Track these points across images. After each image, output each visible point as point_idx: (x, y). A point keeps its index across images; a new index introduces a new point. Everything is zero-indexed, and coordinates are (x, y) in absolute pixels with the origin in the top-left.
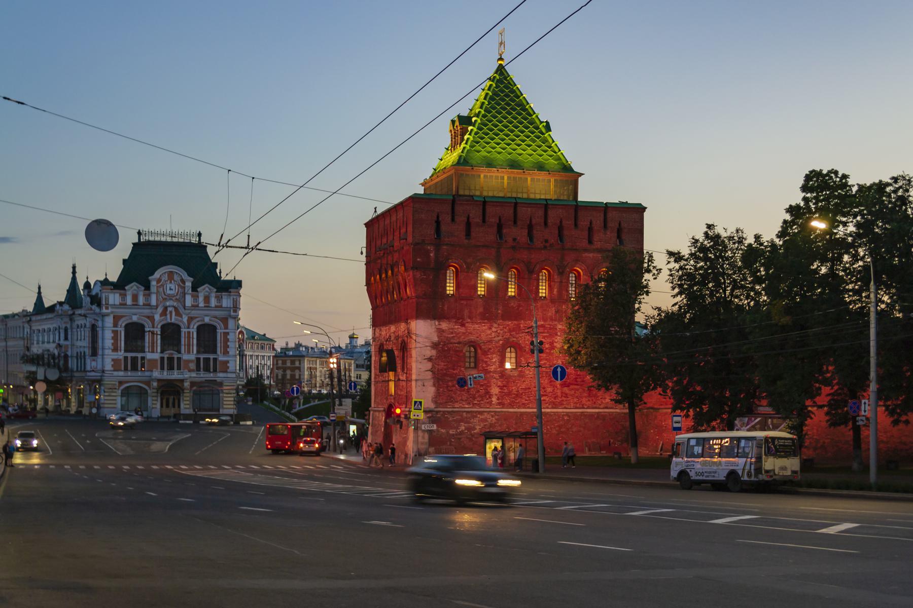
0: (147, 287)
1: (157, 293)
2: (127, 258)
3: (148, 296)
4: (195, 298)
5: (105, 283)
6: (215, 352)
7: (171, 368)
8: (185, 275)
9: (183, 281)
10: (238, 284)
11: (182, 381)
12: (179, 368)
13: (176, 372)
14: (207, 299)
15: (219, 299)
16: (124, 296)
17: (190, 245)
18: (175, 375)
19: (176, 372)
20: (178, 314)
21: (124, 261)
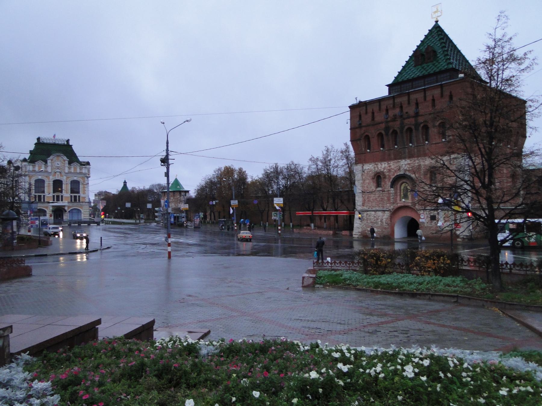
0: (46, 162)
1: (52, 166)
2: (32, 149)
3: (46, 166)
4: (69, 168)
5: (25, 160)
6: (78, 192)
7: (58, 200)
8: (65, 158)
9: (64, 161)
10: (88, 163)
11: (64, 206)
12: (62, 200)
13: (60, 201)
14: (75, 169)
15: (81, 169)
16: (34, 167)
17: (64, 145)
18: (60, 204)
19: (60, 201)
20: (61, 176)
21: (30, 151)
